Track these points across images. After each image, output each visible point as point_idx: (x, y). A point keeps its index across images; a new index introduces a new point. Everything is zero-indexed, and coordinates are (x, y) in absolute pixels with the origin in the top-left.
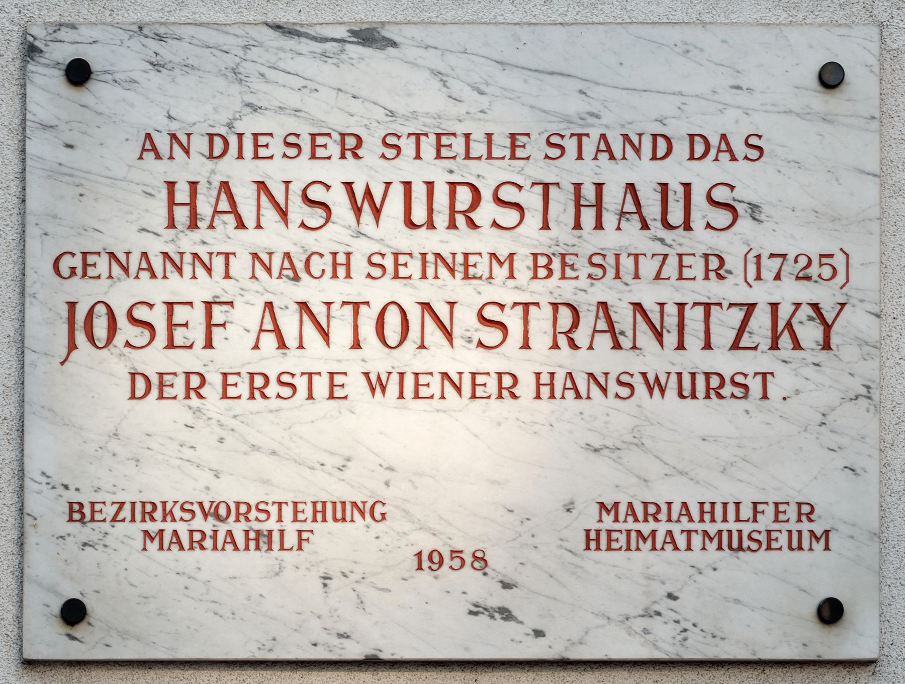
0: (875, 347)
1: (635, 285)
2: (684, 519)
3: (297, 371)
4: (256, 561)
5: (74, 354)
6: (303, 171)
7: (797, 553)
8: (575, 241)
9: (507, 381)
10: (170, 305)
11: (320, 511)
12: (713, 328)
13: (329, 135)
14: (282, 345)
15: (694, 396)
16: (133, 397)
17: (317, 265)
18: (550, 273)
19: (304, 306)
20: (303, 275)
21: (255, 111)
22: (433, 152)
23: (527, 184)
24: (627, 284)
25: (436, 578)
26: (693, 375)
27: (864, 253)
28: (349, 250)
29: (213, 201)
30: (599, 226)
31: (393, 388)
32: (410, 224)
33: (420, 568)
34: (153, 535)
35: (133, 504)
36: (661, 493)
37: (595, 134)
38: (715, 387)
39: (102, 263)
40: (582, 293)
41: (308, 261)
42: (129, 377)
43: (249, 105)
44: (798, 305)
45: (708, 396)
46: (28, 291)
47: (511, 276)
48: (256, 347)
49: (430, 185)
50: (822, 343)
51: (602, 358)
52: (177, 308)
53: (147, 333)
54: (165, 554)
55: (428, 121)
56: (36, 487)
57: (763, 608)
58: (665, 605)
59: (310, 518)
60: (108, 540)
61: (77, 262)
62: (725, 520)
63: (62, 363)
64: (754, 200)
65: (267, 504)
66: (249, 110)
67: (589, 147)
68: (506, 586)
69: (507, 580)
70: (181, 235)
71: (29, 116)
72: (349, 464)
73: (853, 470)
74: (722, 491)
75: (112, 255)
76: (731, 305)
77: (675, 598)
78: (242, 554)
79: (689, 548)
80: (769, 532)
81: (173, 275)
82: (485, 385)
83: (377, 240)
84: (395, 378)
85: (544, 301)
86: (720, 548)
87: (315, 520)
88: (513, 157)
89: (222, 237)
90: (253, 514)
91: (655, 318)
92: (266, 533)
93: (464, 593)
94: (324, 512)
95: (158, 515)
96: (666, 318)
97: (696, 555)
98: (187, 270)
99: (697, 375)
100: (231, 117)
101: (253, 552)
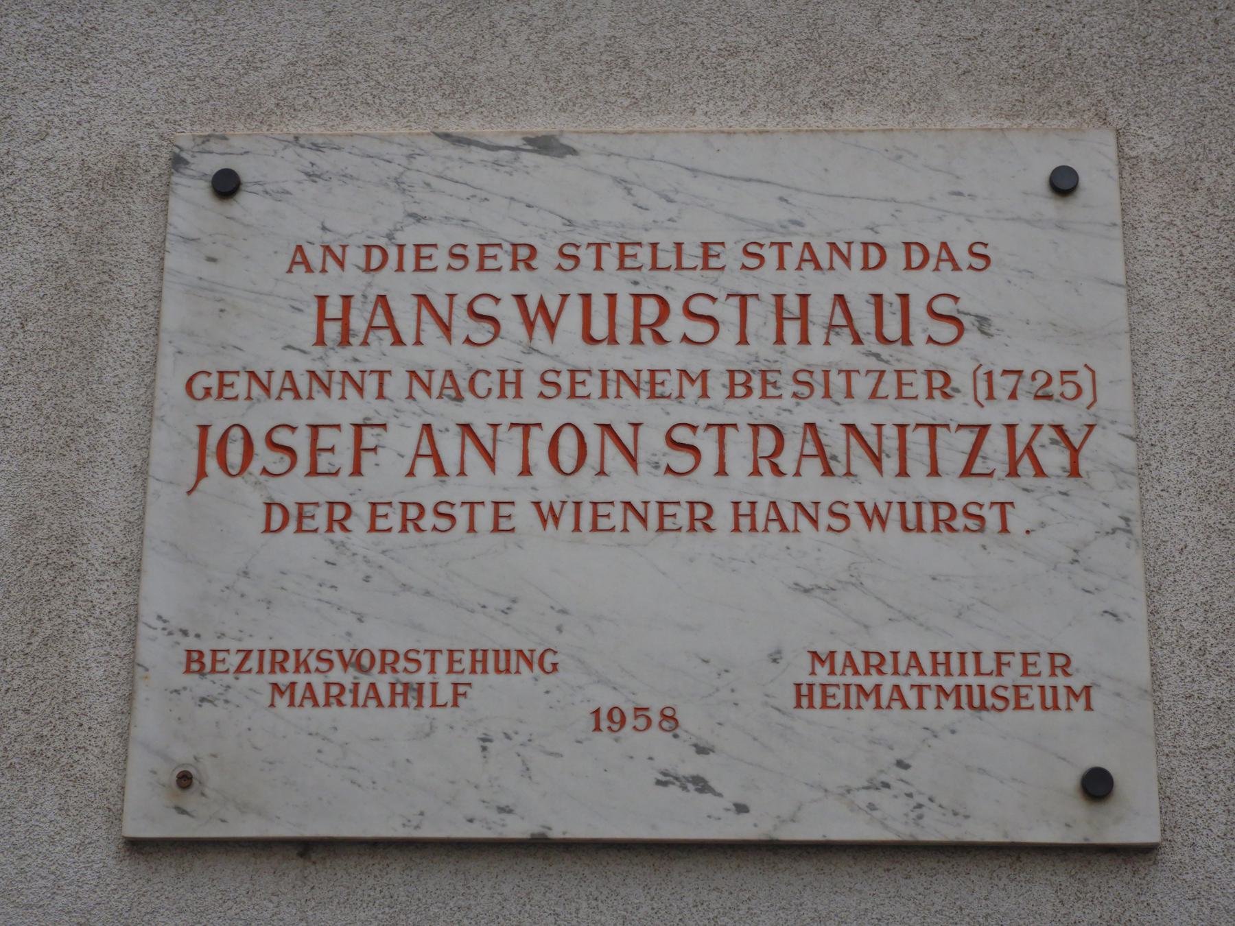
0: (1133, 474)
1: (847, 404)
2: (914, 672)
3: (457, 500)
4: (405, 718)
5: (204, 483)
6: (469, 283)
7: (1051, 713)
8: (777, 356)
9: (700, 512)
10: (315, 428)
11: (479, 660)
12: (940, 452)
13: (500, 245)
14: (440, 471)
15: (920, 528)
17: (482, 383)
18: (749, 391)
19: (466, 428)
20: (467, 395)
21: (419, 221)
22: (616, 263)
23: (721, 296)
24: (838, 404)
25: (617, 740)
26: (919, 505)
27: (1114, 368)
28: (519, 367)
29: (368, 316)
30: (804, 339)
31: (567, 520)
32: (589, 339)
33: (597, 728)
34: (283, 688)
35: (262, 652)
36: (885, 641)
37: (798, 242)
38: (945, 518)
40: (786, 414)
41: (472, 380)
42: (264, 508)
43: (411, 215)
44: (1038, 427)
45: (936, 529)
46: (157, 413)
47: (705, 395)
48: (411, 473)
49: (612, 297)
50: (1068, 466)
51: (811, 485)
52: (322, 431)
53: (287, 460)
54: (296, 711)
55: (611, 230)
56: (151, 632)
57: (1014, 780)
60: (230, 695)
61: (213, 382)
63: (189, 492)
64: (982, 311)
65: (418, 652)
66: (411, 220)
67: (792, 256)
68: (702, 750)
69: (702, 744)
70: (331, 353)
72: (515, 606)
73: (1114, 615)
74: (960, 639)
75: (252, 375)
76: (960, 426)
78: (386, 712)
79: (921, 706)
80: (1017, 688)
81: (320, 396)
82: (674, 515)
83: (551, 357)
84: (570, 508)
85: (742, 422)
86: (958, 706)
87: (473, 671)
88: (706, 267)
91: (872, 440)
92: (416, 686)
93: (651, 758)
94: (484, 661)
95: (290, 665)
96: (885, 441)
97: (929, 715)
98: (336, 390)
99: (924, 506)
100: (392, 228)
101: (400, 711)
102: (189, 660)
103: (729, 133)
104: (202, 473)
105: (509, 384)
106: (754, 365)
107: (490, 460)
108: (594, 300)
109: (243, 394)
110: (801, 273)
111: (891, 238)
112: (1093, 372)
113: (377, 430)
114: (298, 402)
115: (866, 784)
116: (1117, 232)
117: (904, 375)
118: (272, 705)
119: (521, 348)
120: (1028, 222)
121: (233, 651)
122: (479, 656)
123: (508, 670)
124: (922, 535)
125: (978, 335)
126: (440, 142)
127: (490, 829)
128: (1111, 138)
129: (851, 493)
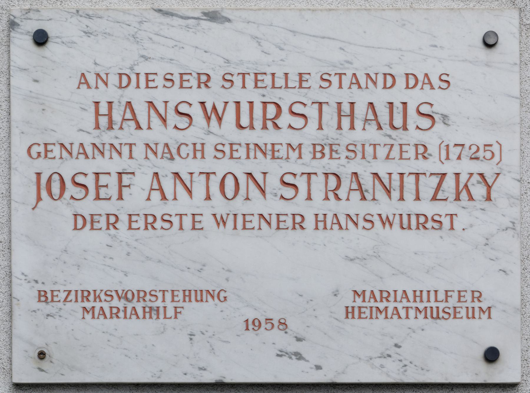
0: (517, 199)
1: (374, 163)
2: (404, 300)
3: (173, 213)
4: (149, 325)
5: (40, 204)
6: (175, 95)
7: (471, 320)
8: (338, 136)
9: (298, 219)
10: (97, 174)
11: (187, 295)
13: (191, 74)
14: (164, 197)
15: (409, 228)
16: (76, 228)
17: (184, 151)
18: (323, 155)
20: (176, 156)
21: (147, 60)
22: (253, 84)
23: (309, 103)
24: (369, 162)
25: (257, 335)
27: (511, 142)
28: (203, 142)
29: (122, 113)
30: (352, 127)
31: (230, 223)
32: (240, 127)
33: (247, 329)
34: (88, 310)
37: (349, 73)
38: (422, 222)
39: (56, 151)
40: (342, 168)
41: (179, 148)
42: (73, 217)
43: (143, 56)
44: (471, 174)
45: (418, 228)
46: (13, 166)
47: (300, 157)
48: (148, 199)
50: (486, 196)
51: (355, 206)
52: (101, 176)
53: (83, 191)
54: (96, 321)
56: (19, 281)
57: (452, 353)
58: (393, 351)
59: (182, 300)
60: (61, 313)
61: (41, 149)
62: (429, 301)
63: (33, 209)
64: (445, 112)
65: (156, 291)
66: (143, 59)
69: (299, 336)
70: (103, 133)
71: (12, 63)
72: (204, 268)
73: (505, 272)
74: (427, 284)
75: (62, 145)
77: (399, 347)
78: (141, 321)
79: (407, 317)
83: (220, 136)
84: (231, 217)
85: (320, 172)
86: (426, 317)
87: (184, 301)
88: (301, 87)
89: (128, 134)
90: (148, 297)
91: (386, 182)
92: (155, 308)
93: (274, 344)
94: (190, 296)
95: (91, 298)
96: (392, 182)
97: (412, 322)
98: (107, 154)
99: (411, 216)
100: (132, 63)
101: (148, 320)
102: (40, 296)
103: (313, 10)
104: (39, 199)
105: (199, 151)
106: (326, 141)
107: (190, 192)
108: (242, 105)
109: (58, 156)
110: (350, 90)
111: (399, 71)
112: (501, 145)
113: (130, 176)
114: (87, 160)
115: (380, 355)
116: (517, 68)
117: (403, 147)
118: (83, 318)
119: (203, 131)
120: (470, 62)
121: (62, 291)
122: (187, 293)
123: (202, 300)
124: (410, 231)
125: (442, 124)
126: (157, 14)
127: (195, 378)
128: (515, 14)
129: (373, 209)
